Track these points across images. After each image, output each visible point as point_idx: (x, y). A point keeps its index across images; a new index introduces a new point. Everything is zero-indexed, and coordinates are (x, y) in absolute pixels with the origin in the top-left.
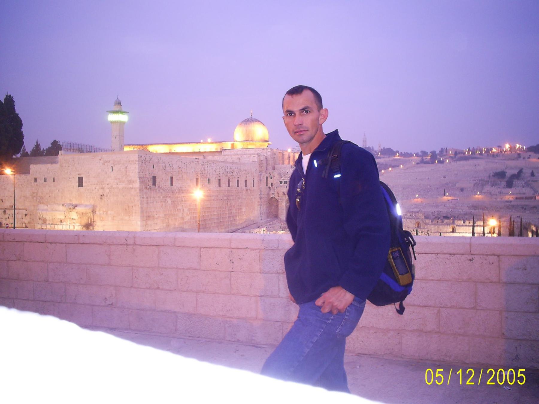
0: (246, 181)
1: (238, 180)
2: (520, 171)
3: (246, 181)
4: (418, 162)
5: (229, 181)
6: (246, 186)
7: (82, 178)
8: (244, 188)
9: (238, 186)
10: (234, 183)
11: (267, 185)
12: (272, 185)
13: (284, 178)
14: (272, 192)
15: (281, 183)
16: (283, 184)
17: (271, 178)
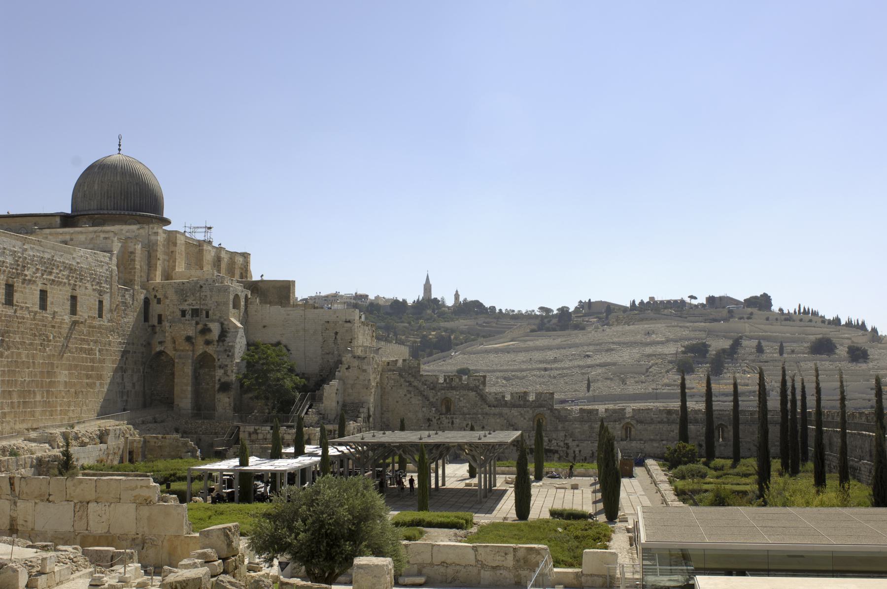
0: (74, 299)
1: (43, 294)
2: (737, 343)
3: (74, 299)
4: (534, 327)
5: (10, 289)
6: (74, 311)
8: (67, 318)
9: (43, 306)
10: (27, 297)
11: (146, 319)
13: (190, 301)
14: (158, 337)
15: (183, 313)
16: (188, 317)
17: (159, 301)
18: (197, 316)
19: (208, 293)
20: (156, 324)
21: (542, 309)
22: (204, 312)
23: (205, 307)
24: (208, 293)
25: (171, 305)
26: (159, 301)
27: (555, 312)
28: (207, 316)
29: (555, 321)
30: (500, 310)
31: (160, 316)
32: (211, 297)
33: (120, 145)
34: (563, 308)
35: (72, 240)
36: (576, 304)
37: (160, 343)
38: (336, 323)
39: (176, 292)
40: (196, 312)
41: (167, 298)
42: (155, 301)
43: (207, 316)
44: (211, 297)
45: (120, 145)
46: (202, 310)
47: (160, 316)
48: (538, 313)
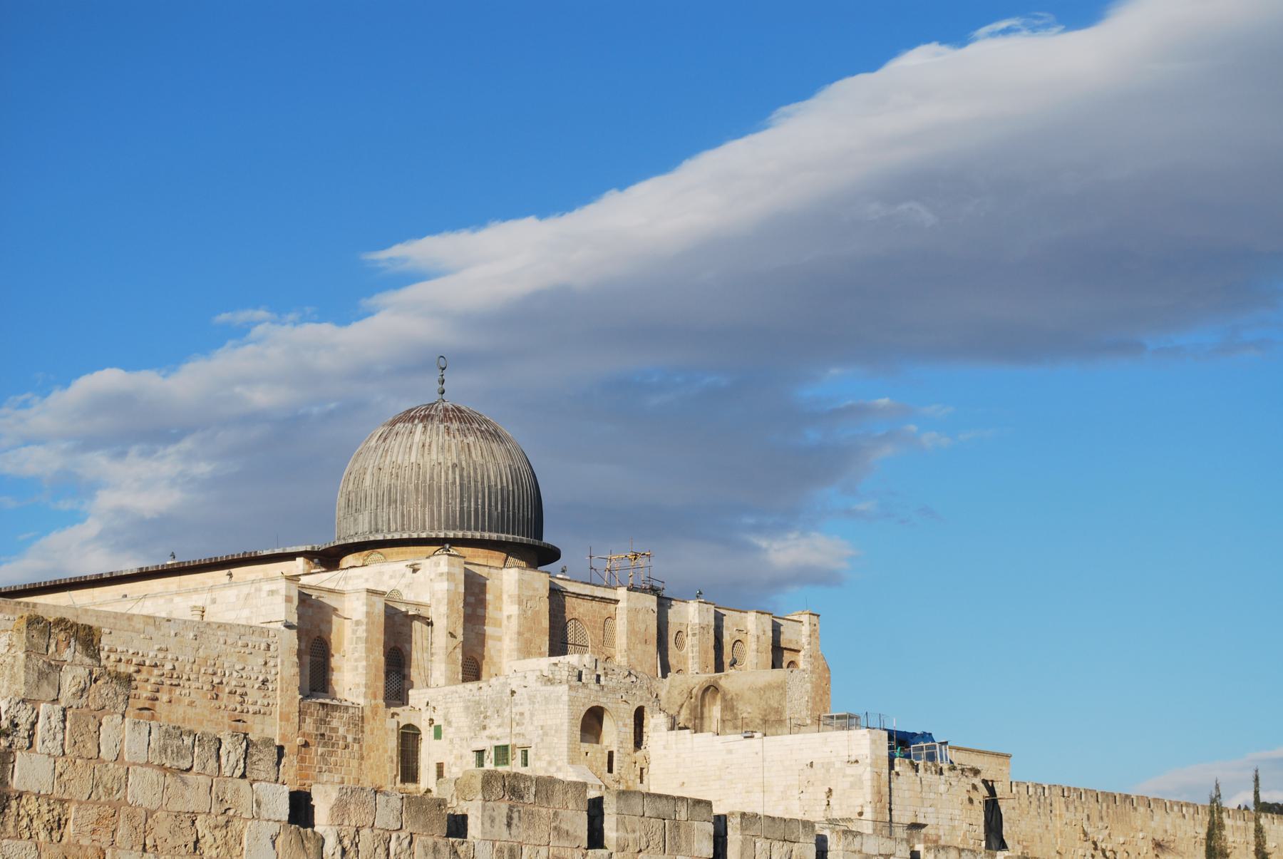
13: (493, 730)
17: (438, 734)
22: (519, 752)
23: (520, 742)
26: (438, 734)
31: (440, 767)
32: (532, 715)
35: (214, 601)
38: (828, 766)
39: (467, 708)
44: (532, 715)
46: (514, 746)
47: (440, 767)
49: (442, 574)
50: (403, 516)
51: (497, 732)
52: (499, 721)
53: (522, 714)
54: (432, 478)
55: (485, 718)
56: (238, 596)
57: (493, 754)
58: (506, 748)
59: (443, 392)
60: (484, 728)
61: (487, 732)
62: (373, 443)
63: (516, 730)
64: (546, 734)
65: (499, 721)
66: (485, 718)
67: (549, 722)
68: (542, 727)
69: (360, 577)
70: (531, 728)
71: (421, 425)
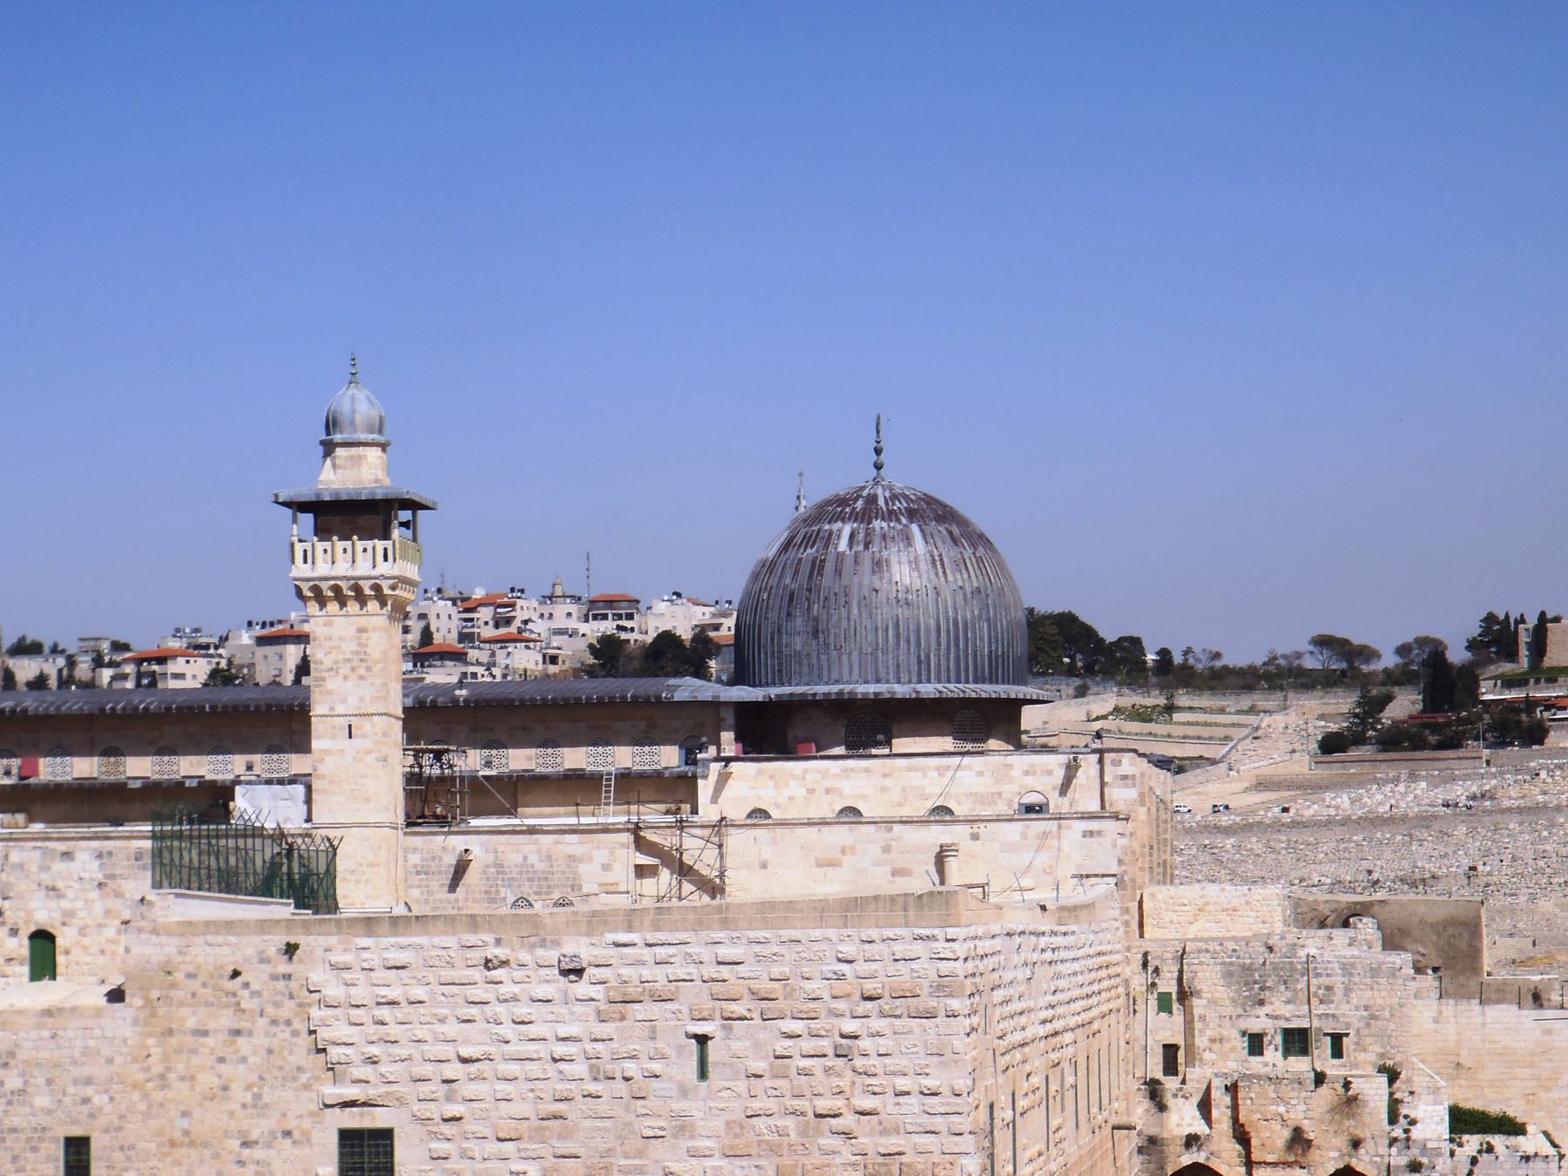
7: (384, 1137)
12: (1171, 1067)
15: (1256, 1044)
16: (1273, 1055)
18: (1304, 1051)
19: (1338, 981)
20: (1159, 1075)
21: (1323, 642)
24: (1338, 981)
25: (1212, 1016)
27: (1389, 661)
28: (1337, 1052)
29: (1404, 705)
30: (1164, 654)
31: (1170, 1051)
32: (1348, 991)
33: (878, 451)
34: (1423, 642)
36: (1475, 630)
37: (1192, 1141)
39: (1228, 975)
40: (1297, 1041)
41: (1198, 994)
42: (1153, 1003)
43: (1337, 1052)
44: (1348, 991)
45: (878, 451)
48: (1309, 663)
49: (1125, 777)
50: (920, 662)
51: (1286, 1010)
52: (1289, 994)
53: (1329, 988)
54: (955, 610)
55: (1262, 989)
56: (1024, 836)
57: (1279, 1039)
58: (1303, 1033)
59: (878, 467)
60: (1261, 1003)
61: (1267, 1009)
62: (843, 545)
63: (1320, 1009)
64: (1373, 1017)
65: (1289, 994)
66: (1262, 989)
67: (1380, 1001)
68: (1366, 1008)
69: (969, 768)
70: (1345, 1008)
71: (915, 528)
